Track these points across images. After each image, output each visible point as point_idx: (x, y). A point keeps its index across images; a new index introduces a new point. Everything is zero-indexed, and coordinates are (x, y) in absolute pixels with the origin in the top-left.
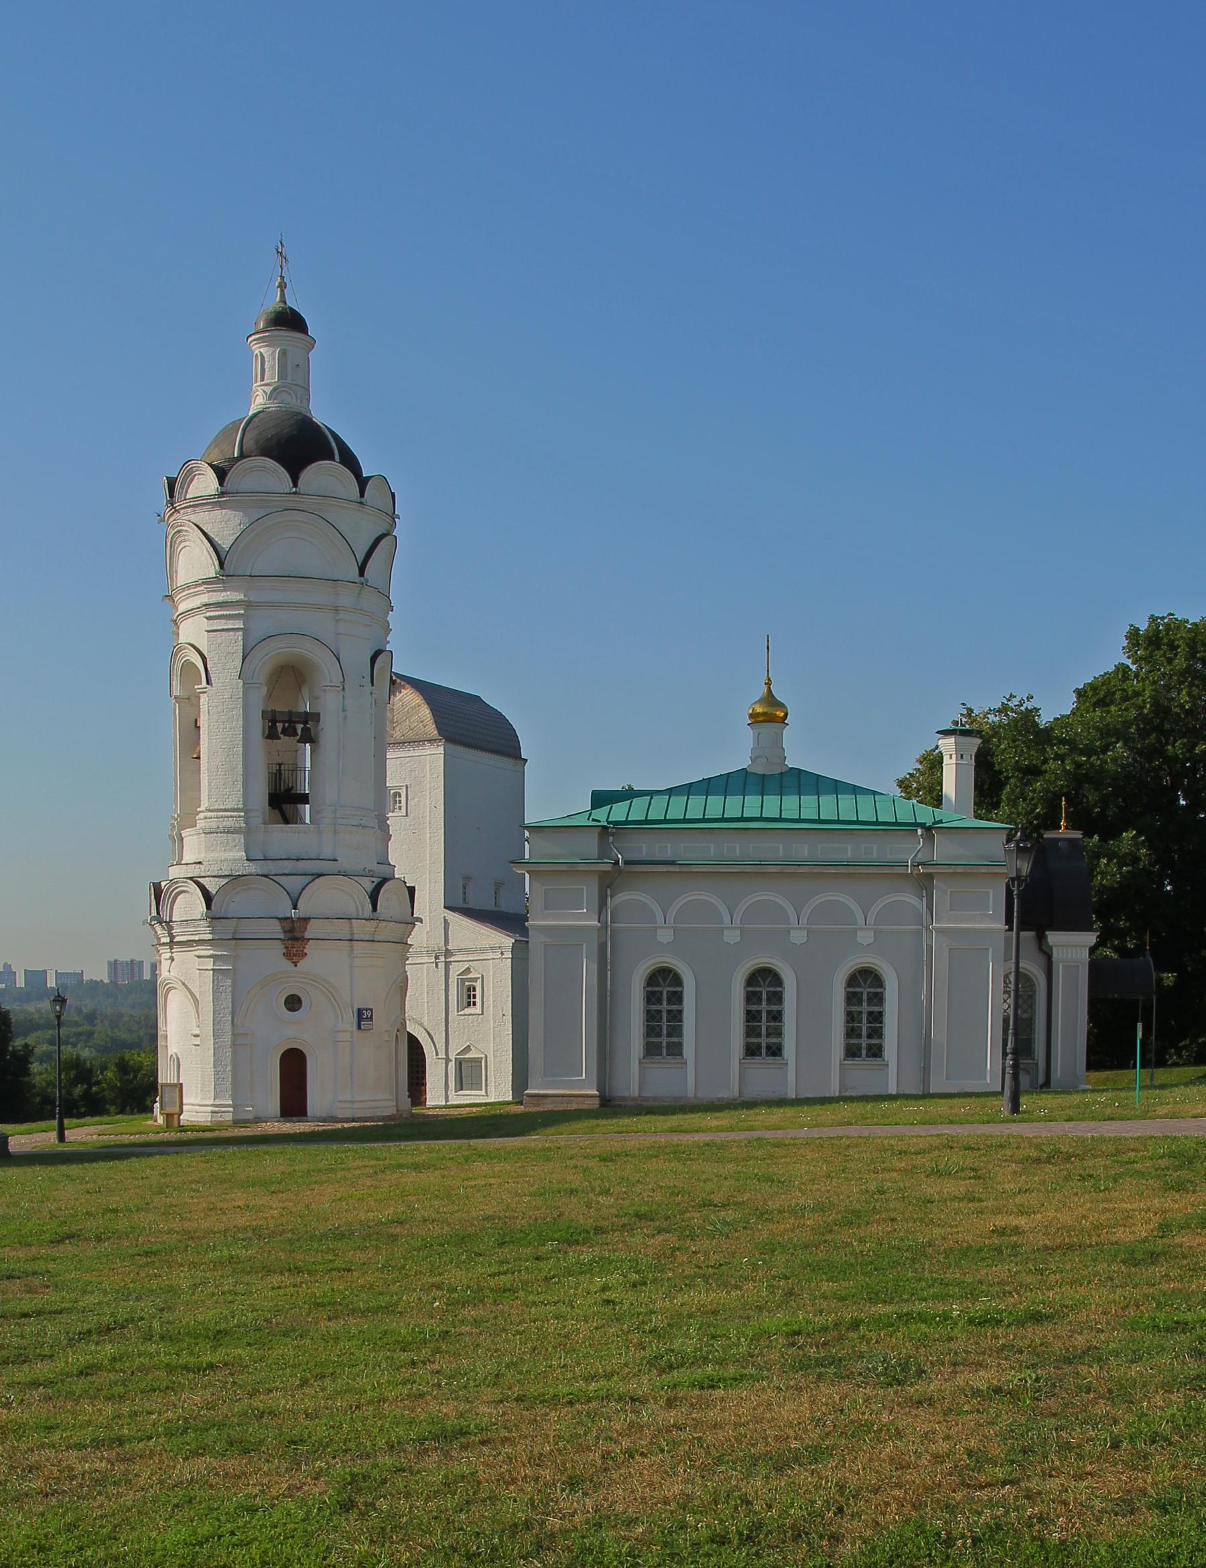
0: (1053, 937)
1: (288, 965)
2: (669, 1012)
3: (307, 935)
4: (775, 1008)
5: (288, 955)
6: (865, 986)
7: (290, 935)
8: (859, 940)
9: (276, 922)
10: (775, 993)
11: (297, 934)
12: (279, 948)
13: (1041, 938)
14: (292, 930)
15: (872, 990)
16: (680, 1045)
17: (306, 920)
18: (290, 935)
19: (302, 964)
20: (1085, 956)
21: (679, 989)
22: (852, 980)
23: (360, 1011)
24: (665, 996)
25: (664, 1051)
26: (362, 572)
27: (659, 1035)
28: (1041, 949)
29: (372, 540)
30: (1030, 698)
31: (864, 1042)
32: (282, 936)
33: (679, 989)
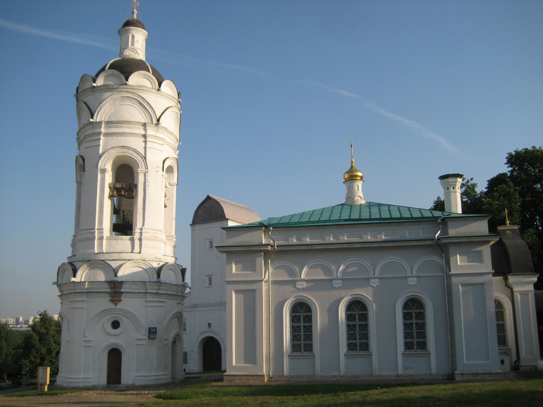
0: (511, 279)
1: (112, 306)
2: (304, 327)
3: (122, 290)
4: (363, 323)
5: (112, 301)
6: (414, 307)
7: (113, 290)
8: (409, 283)
9: (107, 284)
10: (363, 315)
11: (117, 290)
12: (108, 298)
13: (506, 279)
14: (114, 288)
15: (418, 311)
16: (311, 346)
17: (122, 283)
18: (113, 290)
19: (120, 306)
20: (531, 288)
21: (309, 314)
22: (406, 306)
23: (150, 329)
24: (302, 318)
25: (303, 349)
26: (158, 120)
27: (299, 340)
28: (506, 285)
29: (165, 108)
30: (472, 179)
31: (415, 340)
32: (109, 290)
33: (309, 314)
